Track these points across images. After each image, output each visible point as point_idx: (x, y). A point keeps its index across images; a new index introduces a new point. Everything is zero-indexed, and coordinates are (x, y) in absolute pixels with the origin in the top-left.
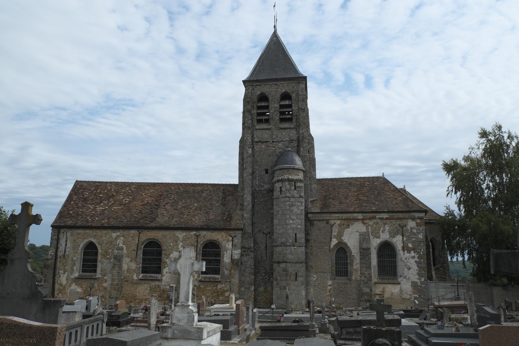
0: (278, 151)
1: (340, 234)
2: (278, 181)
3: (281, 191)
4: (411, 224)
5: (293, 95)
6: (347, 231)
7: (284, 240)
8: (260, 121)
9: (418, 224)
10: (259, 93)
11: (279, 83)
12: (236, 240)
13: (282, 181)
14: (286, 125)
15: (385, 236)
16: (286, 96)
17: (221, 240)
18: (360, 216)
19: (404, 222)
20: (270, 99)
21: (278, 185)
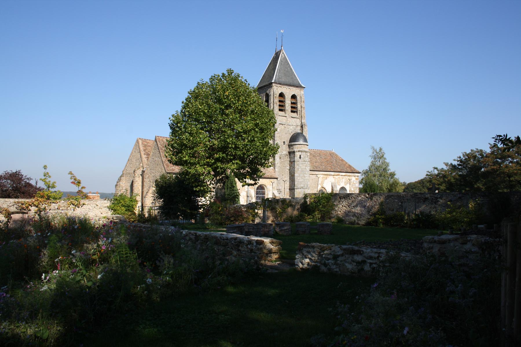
0: (290, 131)
1: (322, 183)
2: (299, 151)
3: (300, 158)
4: (353, 179)
5: (298, 98)
6: (326, 181)
7: (302, 185)
8: (280, 110)
9: (356, 179)
10: (280, 92)
11: (291, 88)
12: (274, 185)
13: (302, 151)
14: (294, 115)
15: (342, 185)
16: (294, 97)
17: (266, 185)
18: (333, 173)
19: (350, 178)
20: (286, 97)
21: (297, 154)
